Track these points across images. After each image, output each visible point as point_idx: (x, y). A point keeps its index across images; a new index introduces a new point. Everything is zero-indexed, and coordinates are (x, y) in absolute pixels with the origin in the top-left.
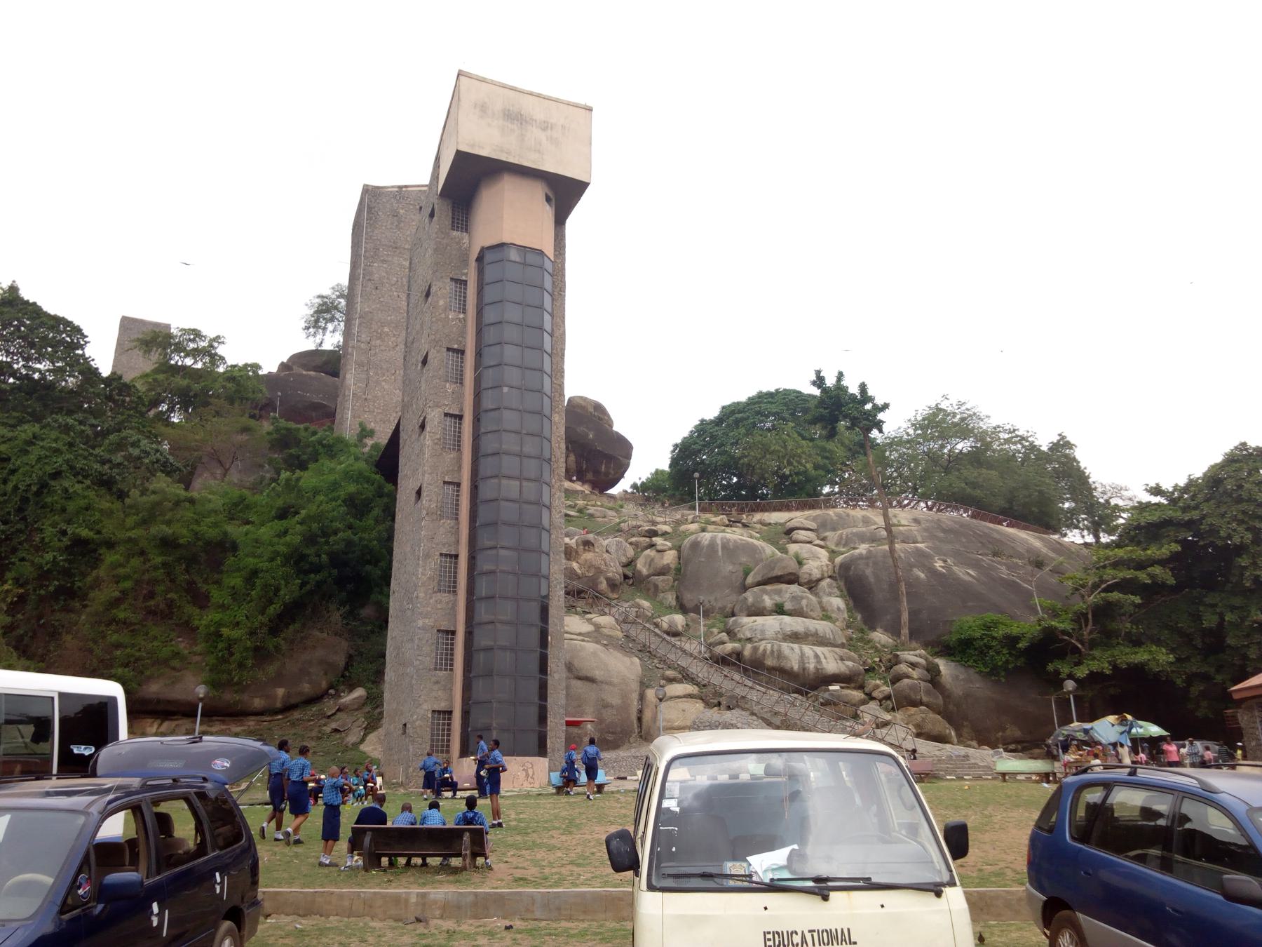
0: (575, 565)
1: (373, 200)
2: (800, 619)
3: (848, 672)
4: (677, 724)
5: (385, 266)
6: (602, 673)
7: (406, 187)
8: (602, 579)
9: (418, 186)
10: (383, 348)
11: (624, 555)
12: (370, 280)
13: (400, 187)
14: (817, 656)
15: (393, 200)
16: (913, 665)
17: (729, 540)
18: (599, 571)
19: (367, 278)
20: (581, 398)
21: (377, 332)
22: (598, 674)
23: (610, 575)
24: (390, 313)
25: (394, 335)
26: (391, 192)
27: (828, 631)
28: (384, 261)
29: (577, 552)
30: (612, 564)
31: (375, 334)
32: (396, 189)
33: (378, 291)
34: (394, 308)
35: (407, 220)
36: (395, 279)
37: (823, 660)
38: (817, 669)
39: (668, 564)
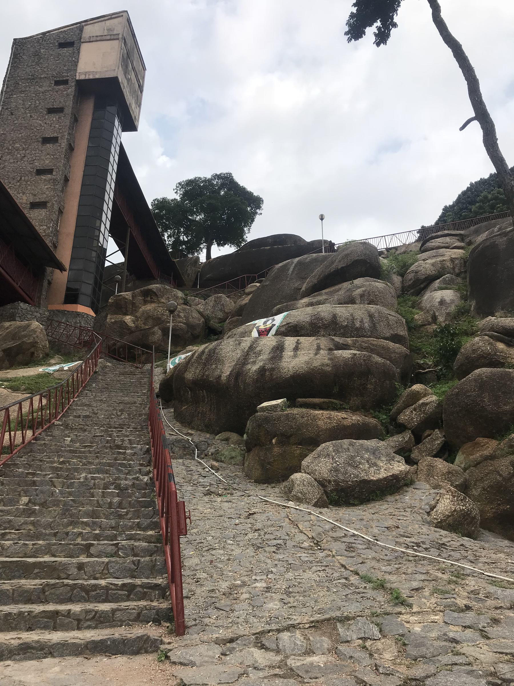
0: (128, 319)
1: (19, 48)
3: (329, 369)
5: (22, 95)
7: (49, 32)
10: (12, 161)
11: (221, 310)
12: (7, 109)
13: (44, 34)
15: (36, 45)
18: (158, 321)
19: (5, 107)
21: (9, 149)
24: (22, 131)
25: (24, 149)
28: (21, 92)
29: (133, 304)
30: (182, 315)
31: (7, 150)
33: (13, 116)
34: (26, 127)
35: (46, 56)
36: (30, 103)
37: (288, 353)
38: (262, 370)
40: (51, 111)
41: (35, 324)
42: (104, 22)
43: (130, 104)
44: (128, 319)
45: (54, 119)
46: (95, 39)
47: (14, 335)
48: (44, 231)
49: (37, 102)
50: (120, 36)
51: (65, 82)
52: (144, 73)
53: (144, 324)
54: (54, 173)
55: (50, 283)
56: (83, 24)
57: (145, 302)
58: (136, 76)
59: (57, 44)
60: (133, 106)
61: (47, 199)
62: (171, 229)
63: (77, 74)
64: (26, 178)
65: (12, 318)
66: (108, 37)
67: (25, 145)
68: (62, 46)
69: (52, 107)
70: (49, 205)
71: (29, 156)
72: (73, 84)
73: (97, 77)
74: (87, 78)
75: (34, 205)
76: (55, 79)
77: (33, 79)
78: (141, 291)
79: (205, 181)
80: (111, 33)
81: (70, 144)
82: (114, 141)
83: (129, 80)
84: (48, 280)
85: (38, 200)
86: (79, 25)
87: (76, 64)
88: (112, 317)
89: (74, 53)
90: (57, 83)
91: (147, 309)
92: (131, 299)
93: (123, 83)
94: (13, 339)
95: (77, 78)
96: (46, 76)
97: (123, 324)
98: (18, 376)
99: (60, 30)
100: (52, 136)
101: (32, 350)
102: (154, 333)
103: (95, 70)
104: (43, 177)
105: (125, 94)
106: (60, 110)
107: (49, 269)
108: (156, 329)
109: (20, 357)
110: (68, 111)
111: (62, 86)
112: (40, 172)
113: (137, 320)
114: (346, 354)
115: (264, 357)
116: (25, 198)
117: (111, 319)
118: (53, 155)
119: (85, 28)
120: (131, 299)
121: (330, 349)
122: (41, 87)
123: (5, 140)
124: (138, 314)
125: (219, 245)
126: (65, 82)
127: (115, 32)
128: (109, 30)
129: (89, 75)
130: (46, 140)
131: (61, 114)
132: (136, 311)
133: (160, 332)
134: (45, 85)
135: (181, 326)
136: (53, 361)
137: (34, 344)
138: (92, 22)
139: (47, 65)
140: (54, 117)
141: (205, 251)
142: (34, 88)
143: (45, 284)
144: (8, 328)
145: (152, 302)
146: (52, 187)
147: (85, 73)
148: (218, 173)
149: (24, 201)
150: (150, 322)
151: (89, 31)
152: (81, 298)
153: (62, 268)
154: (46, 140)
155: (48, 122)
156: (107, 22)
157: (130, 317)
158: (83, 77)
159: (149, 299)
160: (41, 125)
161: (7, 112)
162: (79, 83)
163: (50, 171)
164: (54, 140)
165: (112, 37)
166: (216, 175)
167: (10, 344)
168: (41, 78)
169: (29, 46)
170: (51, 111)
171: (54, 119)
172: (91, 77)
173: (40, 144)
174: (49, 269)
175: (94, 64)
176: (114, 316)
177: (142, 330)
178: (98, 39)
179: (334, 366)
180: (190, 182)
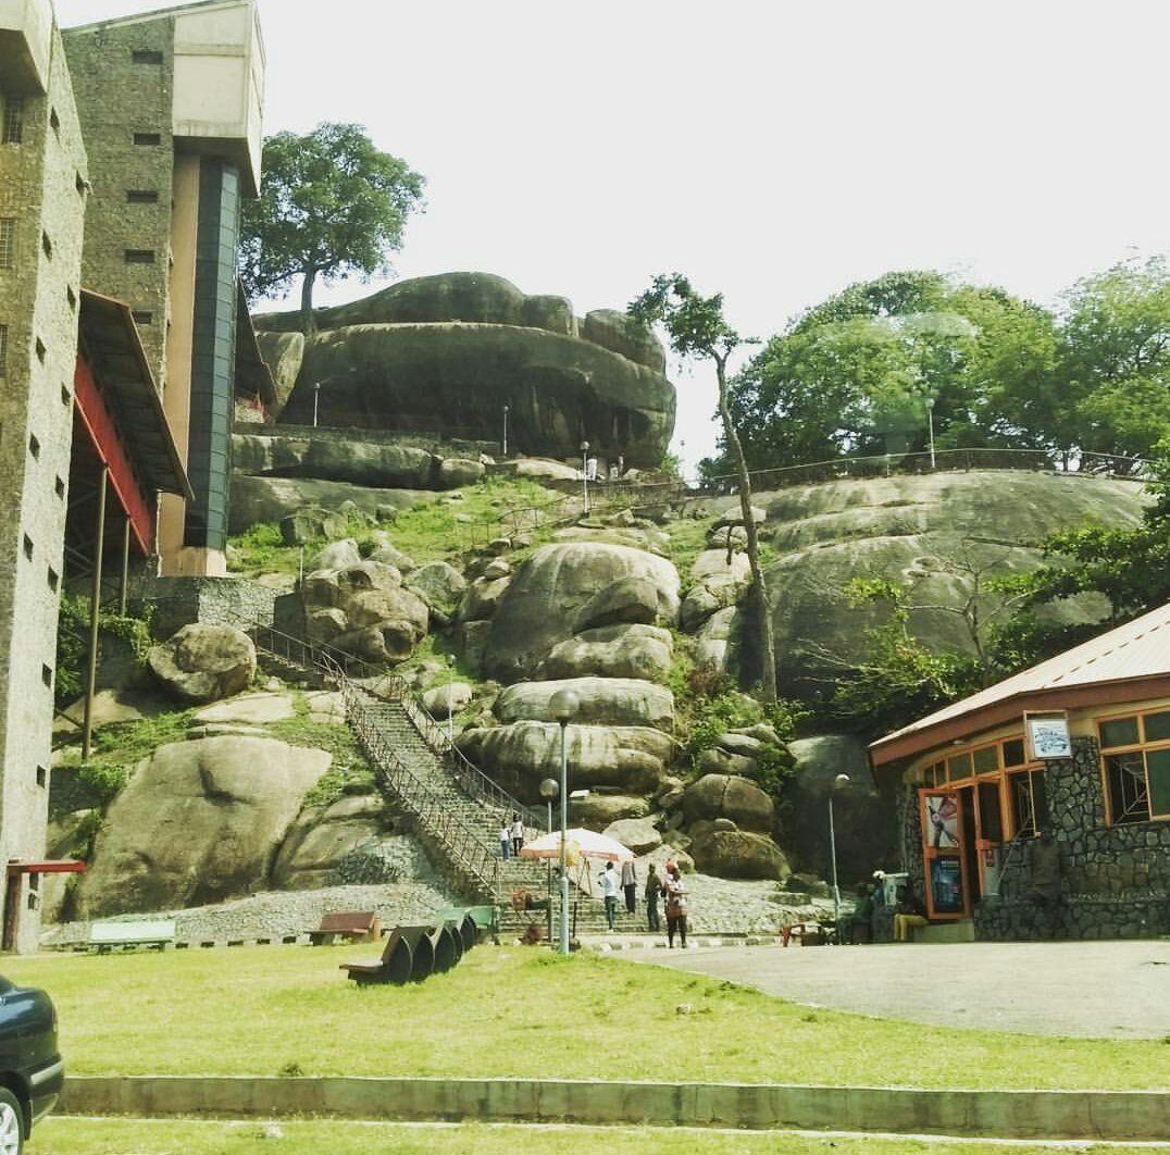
0: (336, 614)
2: (625, 682)
3: (615, 767)
4: (320, 860)
6: (246, 784)
7: (110, 22)
8: (377, 632)
9: (131, 18)
13: (102, 25)
14: (577, 744)
16: (730, 750)
17: (576, 554)
20: (606, 311)
22: (238, 788)
23: (393, 624)
25: (94, 269)
26: (86, 35)
27: (635, 697)
32: (97, 29)
37: (584, 749)
39: (491, 600)
40: (134, 196)
45: (142, 214)
49: (109, 176)
51: (154, 139)
56: (174, 13)
59: (129, 53)
63: (174, 124)
67: (98, 261)
68: (140, 56)
69: (134, 188)
72: (170, 144)
73: (212, 133)
76: (135, 131)
86: (167, 15)
87: (166, 102)
89: (162, 77)
90: (141, 139)
92: (337, 584)
95: (175, 133)
96: (118, 122)
97: (329, 619)
99: (133, 22)
100: (141, 248)
102: (374, 637)
111: (148, 148)
114: (625, 753)
115: (567, 751)
118: (147, 286)
119: (178, 21)
120: (337, 584)
121: (615, 747)
122: (111, 143)
126: (154, 139)
129: (196, 126)
130: (132, 256)
131: (155, 207)
132: (344, 601)
133: (381, 635)
134: (117, 140)
138: (191, 11)
139: (116, 98)
140: (140, 211)
142: (99, 146)
144: (201, 638)
145: (363, 588)
147: (189, 123)
150: (364, 619)
152: (212, 538)
154: (132, 256)
155: (131, 218)
159: (359, 584)
160: (119, 223)
162: (178, 140)
168: (108, 125)
170: (134, 196)
171: (142, 214)
172: (200, 133)
179: (620, 765)
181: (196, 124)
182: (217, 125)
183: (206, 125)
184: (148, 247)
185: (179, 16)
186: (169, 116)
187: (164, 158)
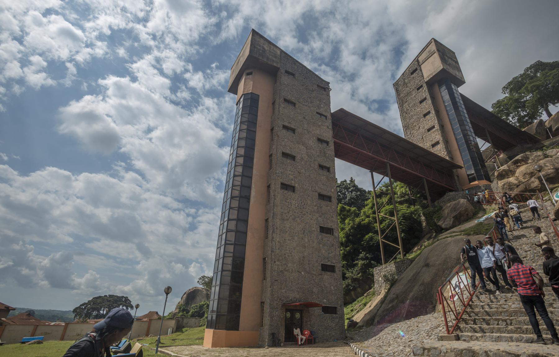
10: (415, 132)
13: (403, 74)
18: (532, 174)
21: (412, 128)
28: (406, 103)
40: (421, 102)
41: (462, 201)
42: (425, 51)
43: (455, 74)
44: (512, 180)
46: (425, 60)
47: (454, 209)
48: (444, 154)
50: (436, 50)
51: (422, 86)
52: (455, 55)
53: (523, 179)
54: (436, 127)
55: (458, 176)
57: (518, 167)
58: (452, 59)
60: (457, 73)
61: (438, 140)
62: (512, 113)
64: (425, 135)
65: (449, 201)
66: (431, 55)
68: (412, 73)
70: (440, 142)
71: (421, 126)
72: (425, 85)
73: (434, 74)
74: (430, 78)
75: (433, 146)
77: (409, 94)
78: (512, 162)
79: (521, 76)
80: (431, 52)
81: (436, 110)
82: (456, 95)
83: (449, 65)
84: (457, 176)
85: (433, 142)
88: (501, 182)
90: (418, 89)
91: (521, 170)
92: (508, 169)
93: (447, 68)
94: (455, 211)
98: (467, 228)
101: (467, 213)
103: (432, 72)
104: (432, 131)
105: (451, 72)
106: (425, 99)
107: (454, 170)
108: (533, 179)
109: (462, 218)
110: (428, 97)
112: (429, 130)
113: (518, 179)
116: (428, 144)
117: (501, 183)
123: (408, 125)
124: (517, 175)
125: (554, 104)
127: (432, 51)
128: (429, 52)
135: (551, 171)
136: (480, 215)
137: (466, 210)
141: (544, 112)
143: (456, 178)
144: (450, 206)
146: (438, 133)
147: (428, 77)
148: (529, 66)
149: (429, 146)
150: (527, 176)
151: (421, 59)
153: (461, 167)
154: (425, 115)
156: (427, 50)
157: (512, 178)
158: (428, 79)
159: (519, 164)
161: (404, 114)
162: (427, 83)
163: (434, 127)
164: (429, 113)
165: (432, 53)
166: (527, 68)
167: (455, 214)
169: (400, 83)
172: (431, 76)
173: (423, 118)
174: (454, 170)
175: (430, 70)
176: (502, 181)
177: (524, 183)
178: (426, 59)
180: (510, 83)
181: (429, 75)
182: (434, 72)
183: (431, 74)
184: (428, 110)
185: (418, 58)
186: (424, 78)
187: (425, 88)
